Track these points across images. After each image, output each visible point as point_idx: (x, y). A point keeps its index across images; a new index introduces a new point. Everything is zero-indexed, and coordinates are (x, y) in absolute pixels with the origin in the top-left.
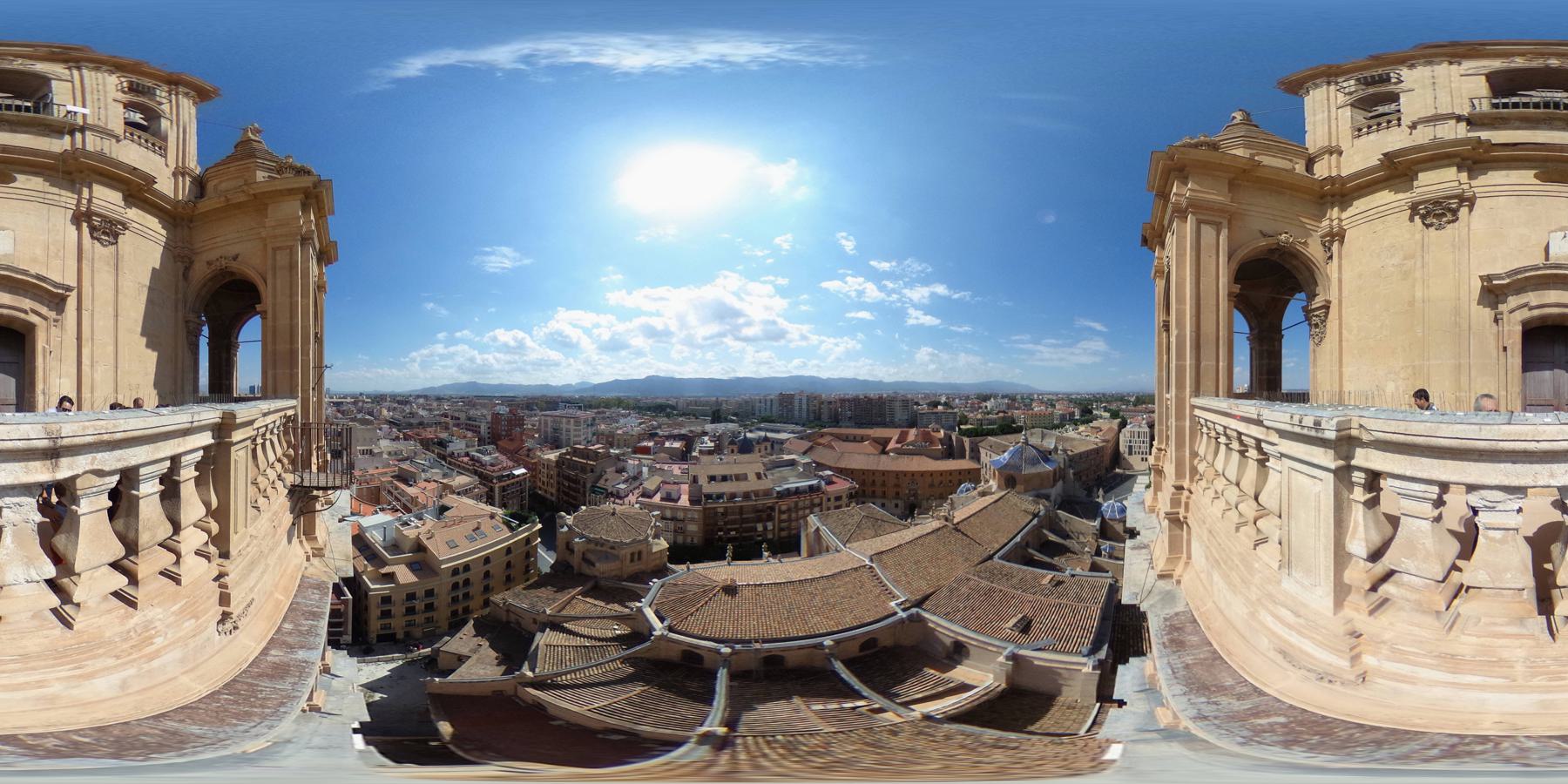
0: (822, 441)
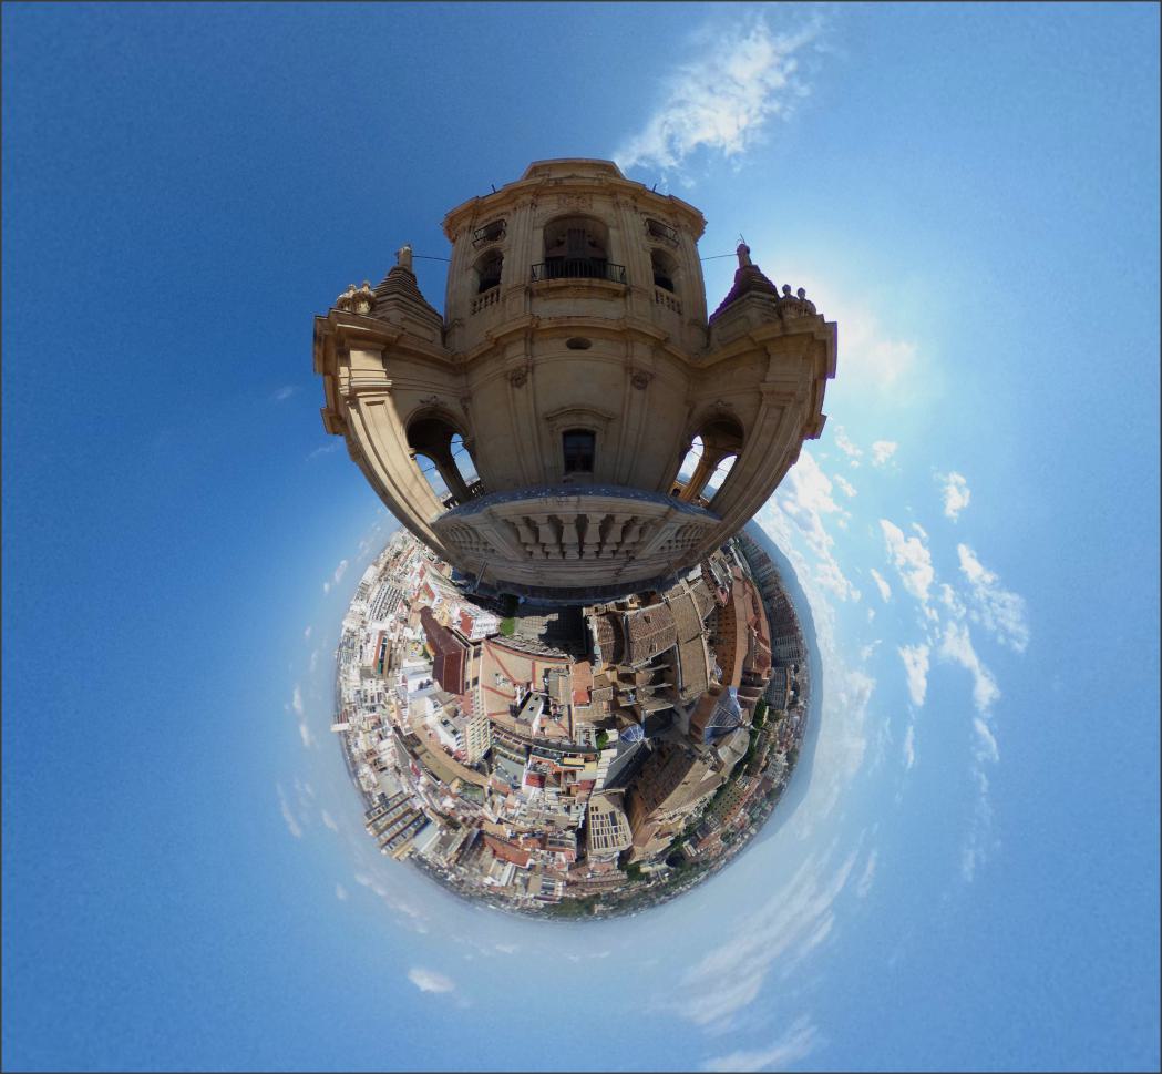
0: (747, 587)
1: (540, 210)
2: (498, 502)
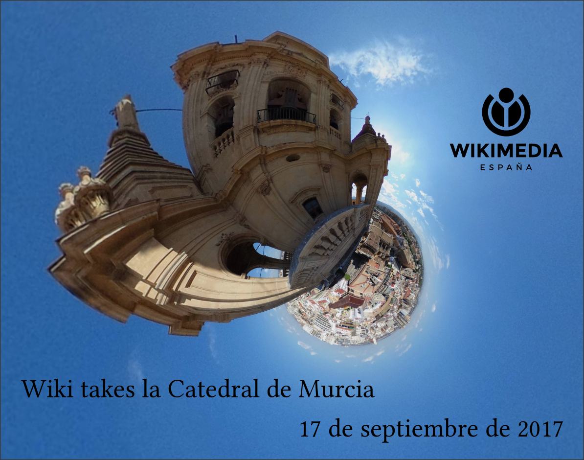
1: (269, 69)
2: (300, 252)
